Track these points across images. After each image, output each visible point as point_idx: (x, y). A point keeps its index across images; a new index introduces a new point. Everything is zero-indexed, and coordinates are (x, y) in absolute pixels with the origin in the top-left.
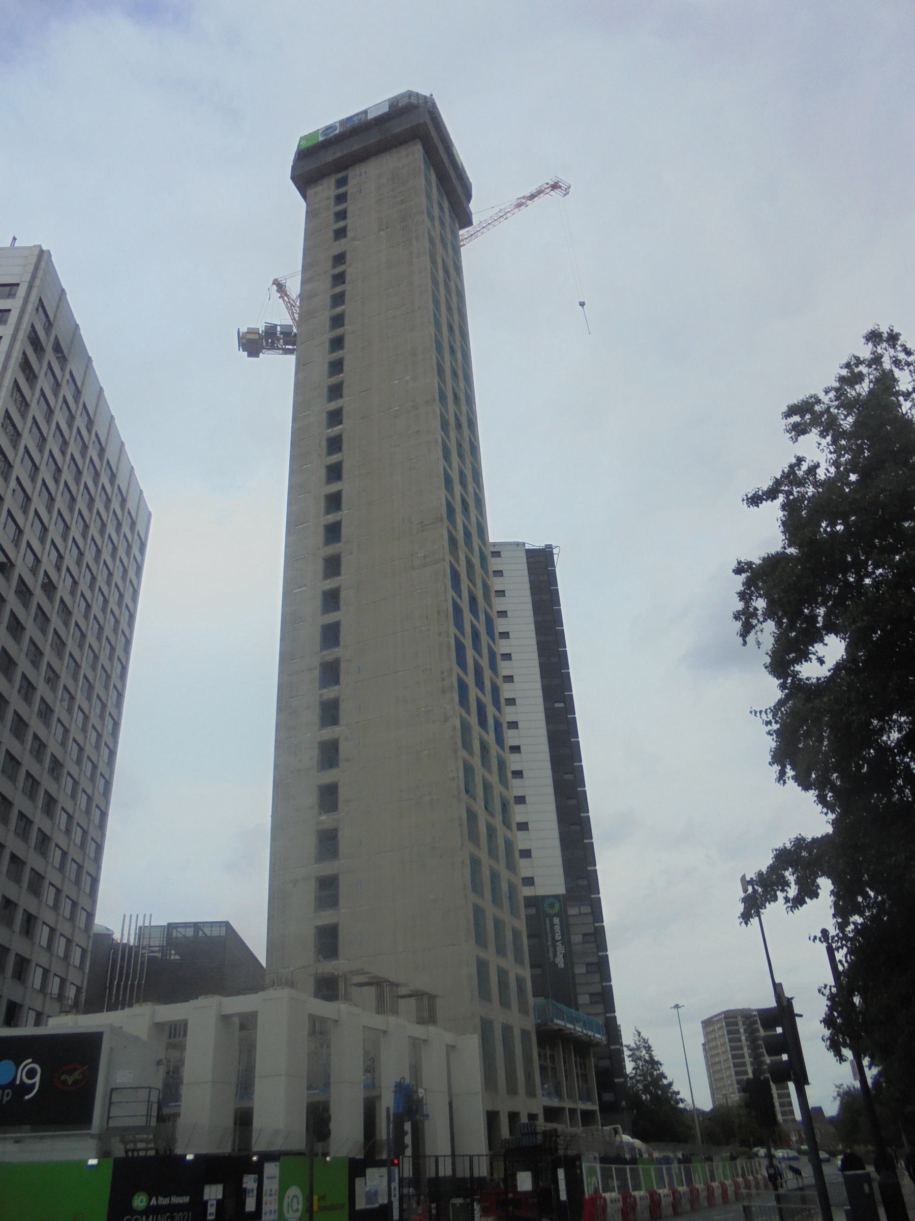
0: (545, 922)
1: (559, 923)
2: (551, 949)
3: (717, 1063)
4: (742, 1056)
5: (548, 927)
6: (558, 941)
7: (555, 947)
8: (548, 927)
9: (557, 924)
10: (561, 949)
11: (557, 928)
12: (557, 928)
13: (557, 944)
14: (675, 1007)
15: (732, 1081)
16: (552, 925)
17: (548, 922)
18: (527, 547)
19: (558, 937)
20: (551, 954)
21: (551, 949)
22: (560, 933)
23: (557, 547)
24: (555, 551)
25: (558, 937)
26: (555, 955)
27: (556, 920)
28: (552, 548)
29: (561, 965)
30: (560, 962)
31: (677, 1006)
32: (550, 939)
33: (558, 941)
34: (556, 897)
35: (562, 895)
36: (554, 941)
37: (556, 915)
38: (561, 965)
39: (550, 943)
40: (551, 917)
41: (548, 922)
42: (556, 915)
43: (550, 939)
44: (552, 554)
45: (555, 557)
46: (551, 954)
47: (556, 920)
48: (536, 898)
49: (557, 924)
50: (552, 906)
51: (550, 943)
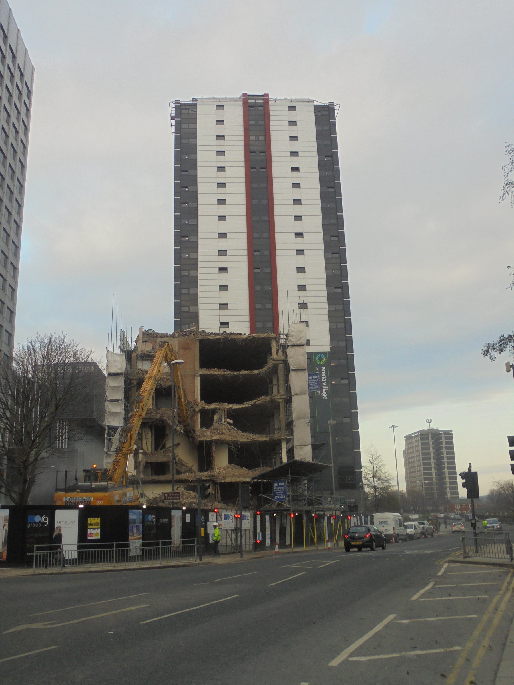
1: (325, 370)
3: (412, 462)
4: (429, 459)
6: (324, 382)
9: (324, 371)
11: (324, 374)
13: (323, 384)
14: (392, 427)
15: (421, 473)
17: (317, 369)
18: (315, 103)
22: (325, 377)
23: (337, 104)
24: (336, 108)
25: (324, 379)
27: (323, 369)
28: (333, 105)
29: (325, 398)
31: (393, 426)
33: (324, 382)
34: (324, 353)
37: (323, 365)
38: (325, 398)
40: (320, 366)
41: (317, 369)
42: (323, 365)
44: (333, 110)
45: (336, 112)
47: (323, 369)
49: (324, 371)
50: (321, 359)
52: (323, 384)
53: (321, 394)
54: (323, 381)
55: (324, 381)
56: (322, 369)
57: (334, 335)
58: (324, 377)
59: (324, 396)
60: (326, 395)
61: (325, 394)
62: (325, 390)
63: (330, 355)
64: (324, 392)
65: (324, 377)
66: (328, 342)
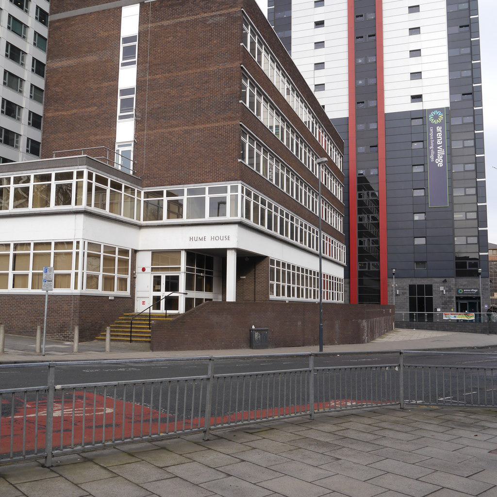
0: (429, 129)
1: (441, 131)
2: (433, 152)
5: (432, 135)
6: (440, 145)
7: (436, 150)
8: (432, 135)
9: (440, 132)
10: (441, 152)
11: (439, 135)
12: (439, 135)
13: (438, 148)
16: (435, 132)
17: (431, 130)
19: (439, 142)
20: (432, 157)
21: (433, 152)
22: (441, 139)
25: (439, 142)
26: (436, 157)
27: (439, 129)
29: (441, 165)
30: (440, 162)
32: (432, 144)
33: (440, 145)
34: (441, 110)
35: (447, 108)
36: (436, 146)
37: (439, 125)
38: (441, 165)
39: (432, 147)
40: (435, 126)
41: (431, 130)
42: (439, 125)
43: (432, 144)
46: (432, 157)
47: (439, 129)
48: (424, 111)
49: (440, 132)
50: (436, 117)
51: (432, 147)
52: (438, 148)
53: (435, 160)
54: (438, 144)
55: (440, 143)
56: (438, 129)
57: (454, 85)
58: (440, 139)
59: (439, 163)
60: (442, 162)
61: (441, 161)
62: (441, 155)
63: (449, 113)
64: (439, 158)
65: (440, 139)
66: (447, 95)
